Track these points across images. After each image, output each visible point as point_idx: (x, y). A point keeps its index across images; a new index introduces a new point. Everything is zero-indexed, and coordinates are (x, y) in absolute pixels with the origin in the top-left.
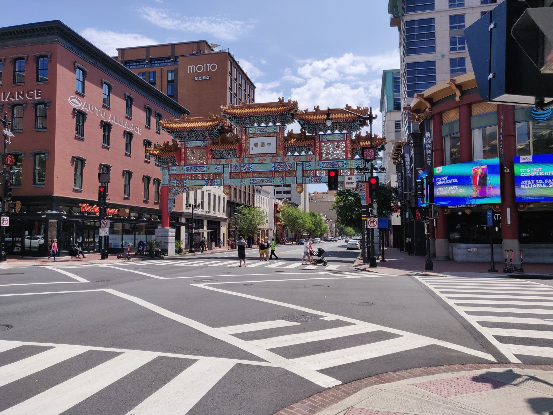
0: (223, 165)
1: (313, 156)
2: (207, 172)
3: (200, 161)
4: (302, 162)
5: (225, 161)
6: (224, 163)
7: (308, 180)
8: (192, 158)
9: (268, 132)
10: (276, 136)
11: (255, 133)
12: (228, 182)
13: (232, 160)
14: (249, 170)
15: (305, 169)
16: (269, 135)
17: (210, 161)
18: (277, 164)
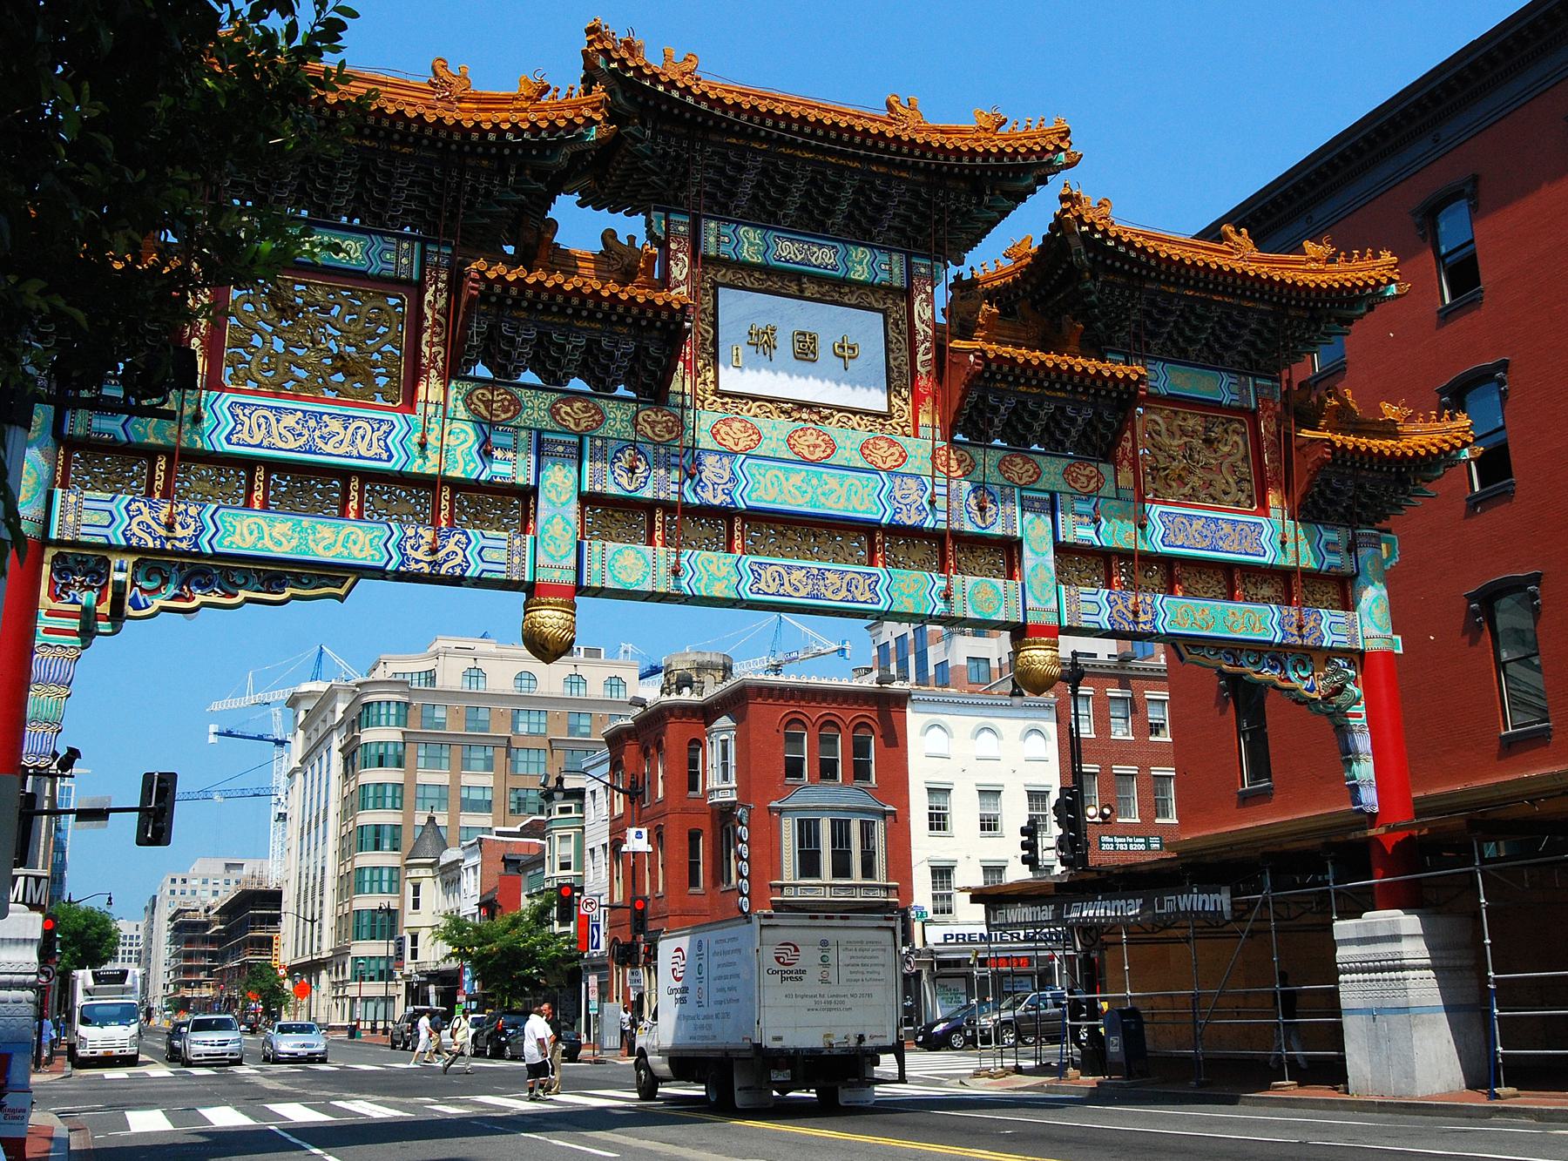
0: (540, 432)
1: (1106, 469)
2: (416, 466)
3: (339, 377)
4: (1053, 495)
5: (553, 412)
6: (547, 422)
7: (1093, 608)
8: (279, 345)
9: (840, 273)
10: (885, 313)
11: (758, 259)
12: (572, 561)
13: (599, 411)
14: (729, 494)
15: (1070, 539)
16: (835, 290)
17: (431, 390)
18: (911, 483)
